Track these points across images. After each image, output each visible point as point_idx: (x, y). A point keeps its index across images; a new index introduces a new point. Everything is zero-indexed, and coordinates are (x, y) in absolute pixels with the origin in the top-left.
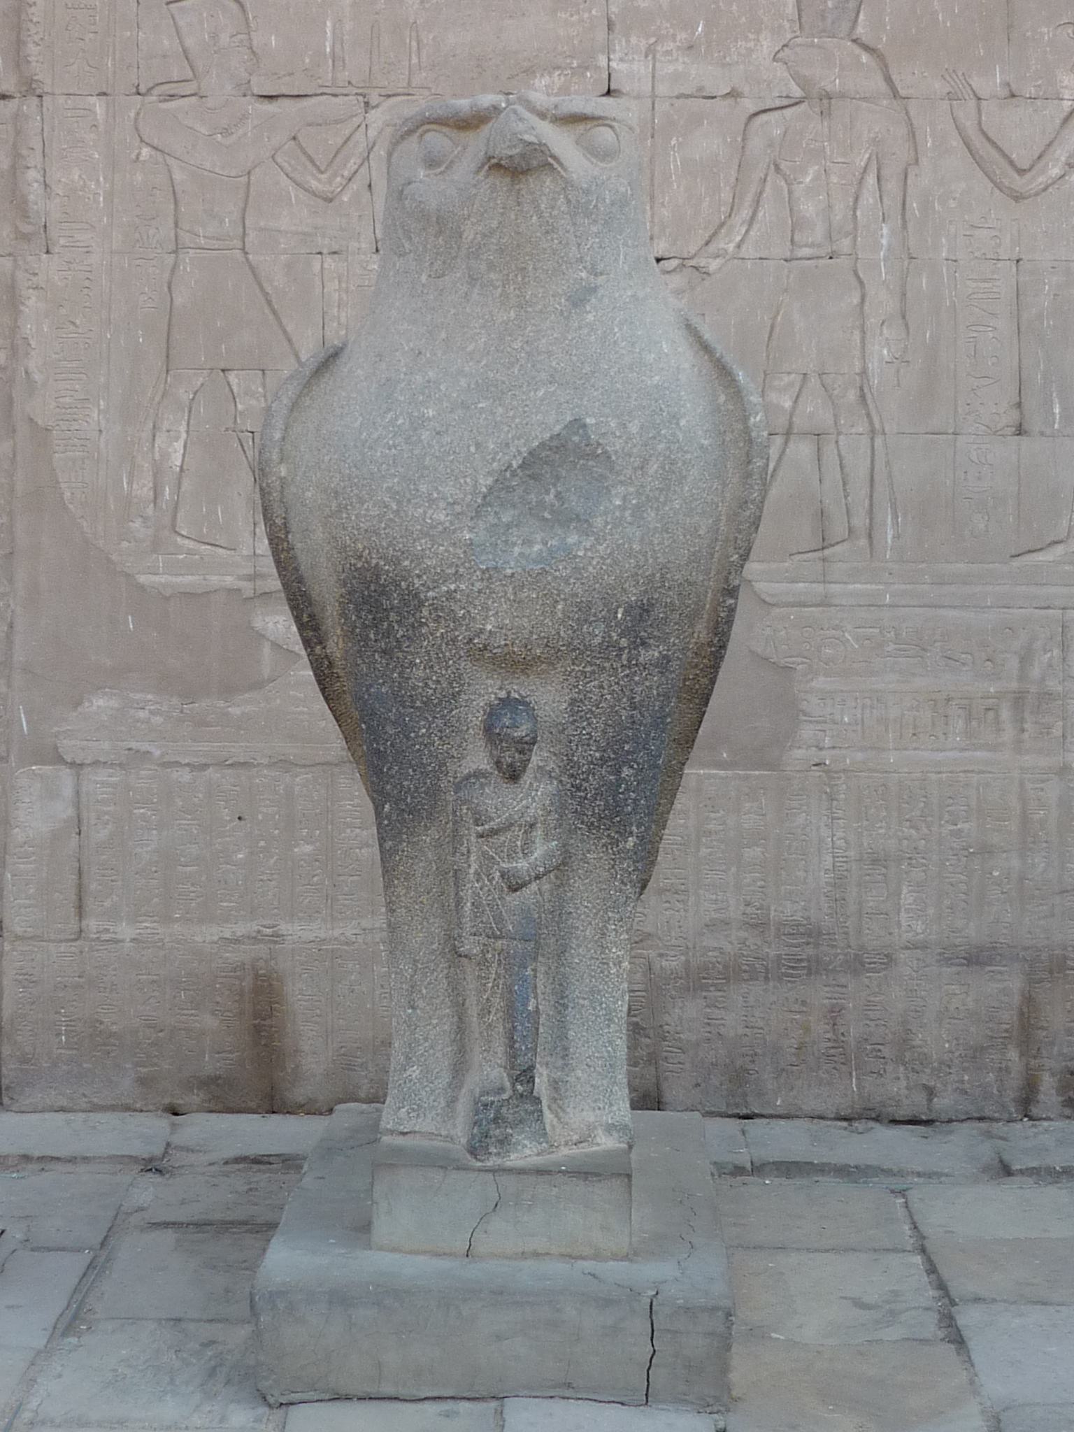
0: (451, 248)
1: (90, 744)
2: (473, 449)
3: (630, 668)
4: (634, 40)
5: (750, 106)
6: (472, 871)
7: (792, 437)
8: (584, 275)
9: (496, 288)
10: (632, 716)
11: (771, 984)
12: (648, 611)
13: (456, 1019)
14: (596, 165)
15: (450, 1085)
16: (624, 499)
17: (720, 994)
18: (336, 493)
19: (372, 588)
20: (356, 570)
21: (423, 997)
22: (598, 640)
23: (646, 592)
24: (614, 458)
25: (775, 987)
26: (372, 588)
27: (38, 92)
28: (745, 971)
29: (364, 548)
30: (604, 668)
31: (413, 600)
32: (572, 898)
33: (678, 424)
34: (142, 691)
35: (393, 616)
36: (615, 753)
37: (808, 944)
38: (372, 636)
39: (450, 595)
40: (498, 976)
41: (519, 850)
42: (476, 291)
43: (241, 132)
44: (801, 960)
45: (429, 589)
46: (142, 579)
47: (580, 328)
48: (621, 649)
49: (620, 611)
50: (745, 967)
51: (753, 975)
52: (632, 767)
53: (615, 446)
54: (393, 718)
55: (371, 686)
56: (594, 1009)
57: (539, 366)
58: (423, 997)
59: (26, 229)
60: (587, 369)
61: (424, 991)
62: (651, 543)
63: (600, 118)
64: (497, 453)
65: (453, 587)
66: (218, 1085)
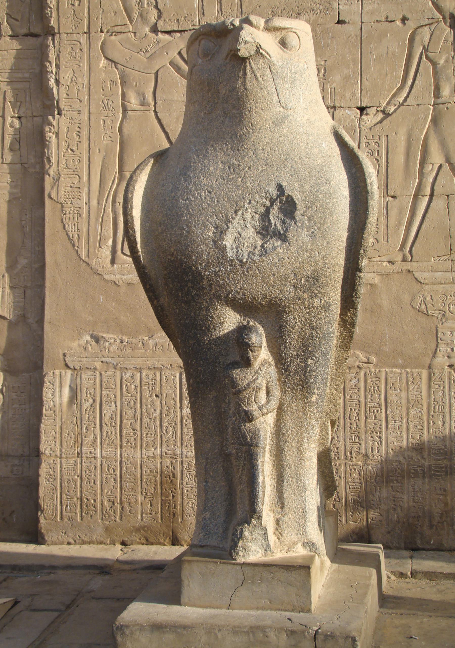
0: (215, 98)
1: (82, 359)
2: (226, 199)
3: (309, 309)
5: (411, 25)
6: (231, 412)
7: (434, 197)
8: (282, 109)
9: (237, 118)
10: (312, 333)
11: (426, 480)
12: (317, 280)
13: (227, 488)
14: (287, 53)
15: (225, 521)
16: (303, 223)
17: (399, 485)
18: (160, 223)
19: (179, 270)
20: (171, 261)
21: (211, 477)
22: (292, 294)
23: (316, 270)
24: (297, 202)
25: (429, 482)
26: (179, 270)
27: (52, 32)
28: (413, 473)
29: (175, 250)
30: (296, 309)
31: (198, 277)
32: (284, 426)
33: (330, 184)
34: (108, 333)
35: (190, 285)
36: (303, 352)
37: (445, 459)
38: (180, 294)
39: (216, 274)
40: (244, 465)
41: (253, 401)
42: (227, 119)
43: (153, 51)
44: (442, 467)
45: (206, 271)
46: (107, 277)
47: (280, 137)
48: (304, 299)
49: (303, 280)
50: (412, 471)
51: (416, 474)
52: (312, 359)
53: (297, 197)
54: (192, 336)
55: (181, 320)
56: (297, 483)
57: (259, 157)
58: (211, 477)
59: (48, 103)
60: (283, 157)
61: (211, 474)
62: (317, 245)
63: (288, 28)
64: (238, 201)
65: (217, 269)
66: (145, 531)
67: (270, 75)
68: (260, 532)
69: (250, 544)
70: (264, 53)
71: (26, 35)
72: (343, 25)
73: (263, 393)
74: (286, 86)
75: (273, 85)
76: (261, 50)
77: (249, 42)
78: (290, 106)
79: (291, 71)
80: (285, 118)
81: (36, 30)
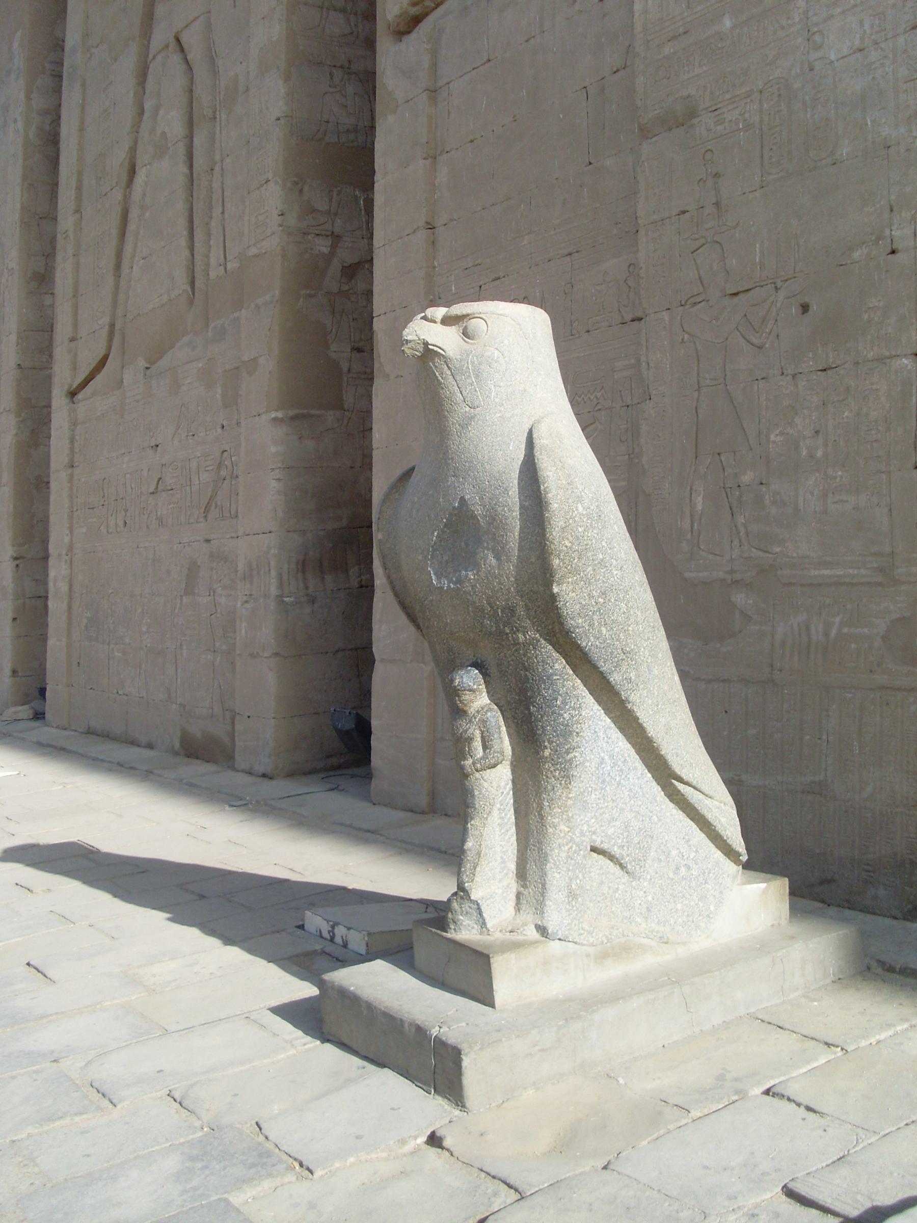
4: (903, 214)
8: (467, 409)
23: (508, 600)
48: (507, 634)
53: (479, 511)
63: (468, 315)
67: (449, 372)
68: (471, 905)
69: (461, 917)
70: (435, 349)
71: (633, 320)
72: (898, 255)
73: (477, 744)
74: (469, 381)
75: (454, 383)
76: (430, 347)
77: (410, 341)
78: (476, 403)
79: (473, 363)
80: (471, 418)
81: (639, 314)
